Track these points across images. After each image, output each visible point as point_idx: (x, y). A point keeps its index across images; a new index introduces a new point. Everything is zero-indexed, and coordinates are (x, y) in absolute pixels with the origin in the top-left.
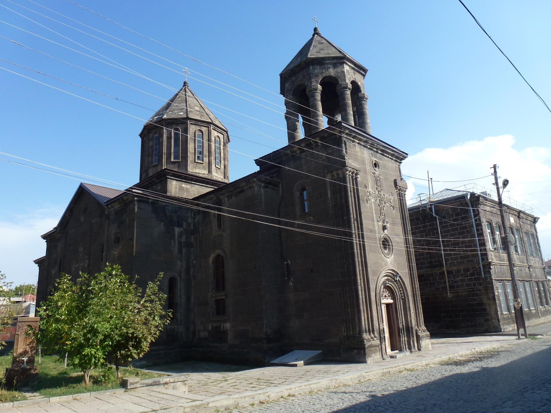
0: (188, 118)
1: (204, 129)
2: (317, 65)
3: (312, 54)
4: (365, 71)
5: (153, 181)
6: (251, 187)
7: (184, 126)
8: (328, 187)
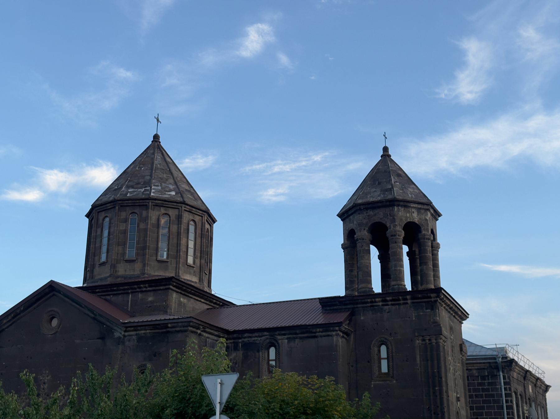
0: (184, 203)
1: (197, 218)
2: (402, 206)
3: (398, 193)
4: (439, 215)
5: (140, 288)
6: (328, 336)
7: (176, 212)
8: (418, 352)
